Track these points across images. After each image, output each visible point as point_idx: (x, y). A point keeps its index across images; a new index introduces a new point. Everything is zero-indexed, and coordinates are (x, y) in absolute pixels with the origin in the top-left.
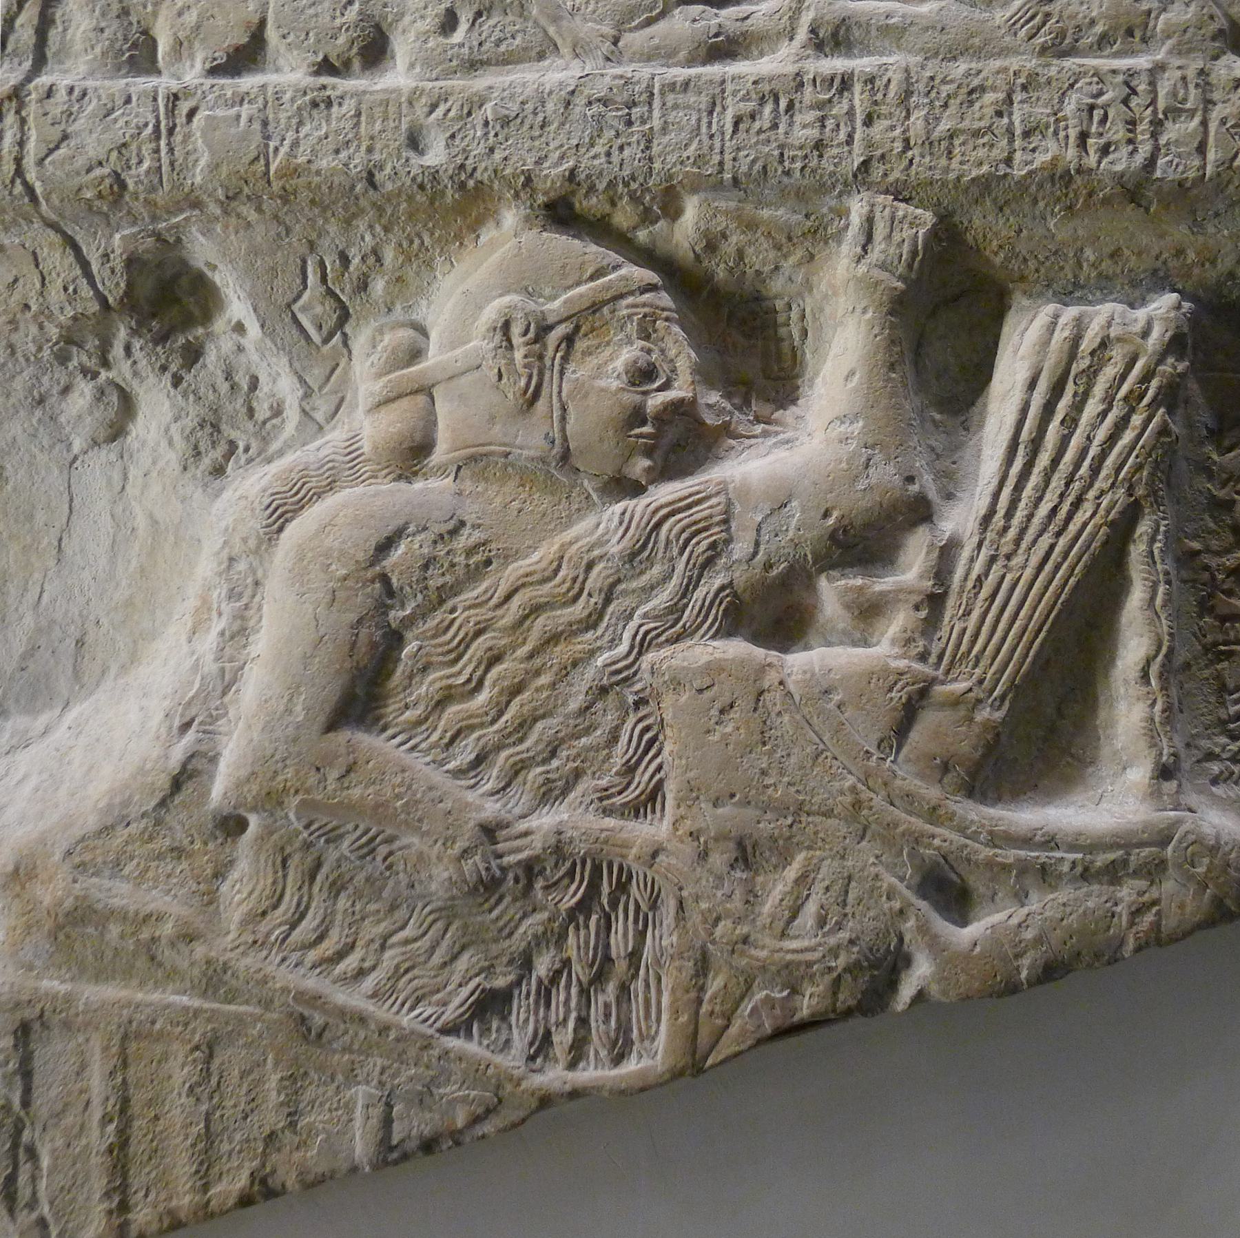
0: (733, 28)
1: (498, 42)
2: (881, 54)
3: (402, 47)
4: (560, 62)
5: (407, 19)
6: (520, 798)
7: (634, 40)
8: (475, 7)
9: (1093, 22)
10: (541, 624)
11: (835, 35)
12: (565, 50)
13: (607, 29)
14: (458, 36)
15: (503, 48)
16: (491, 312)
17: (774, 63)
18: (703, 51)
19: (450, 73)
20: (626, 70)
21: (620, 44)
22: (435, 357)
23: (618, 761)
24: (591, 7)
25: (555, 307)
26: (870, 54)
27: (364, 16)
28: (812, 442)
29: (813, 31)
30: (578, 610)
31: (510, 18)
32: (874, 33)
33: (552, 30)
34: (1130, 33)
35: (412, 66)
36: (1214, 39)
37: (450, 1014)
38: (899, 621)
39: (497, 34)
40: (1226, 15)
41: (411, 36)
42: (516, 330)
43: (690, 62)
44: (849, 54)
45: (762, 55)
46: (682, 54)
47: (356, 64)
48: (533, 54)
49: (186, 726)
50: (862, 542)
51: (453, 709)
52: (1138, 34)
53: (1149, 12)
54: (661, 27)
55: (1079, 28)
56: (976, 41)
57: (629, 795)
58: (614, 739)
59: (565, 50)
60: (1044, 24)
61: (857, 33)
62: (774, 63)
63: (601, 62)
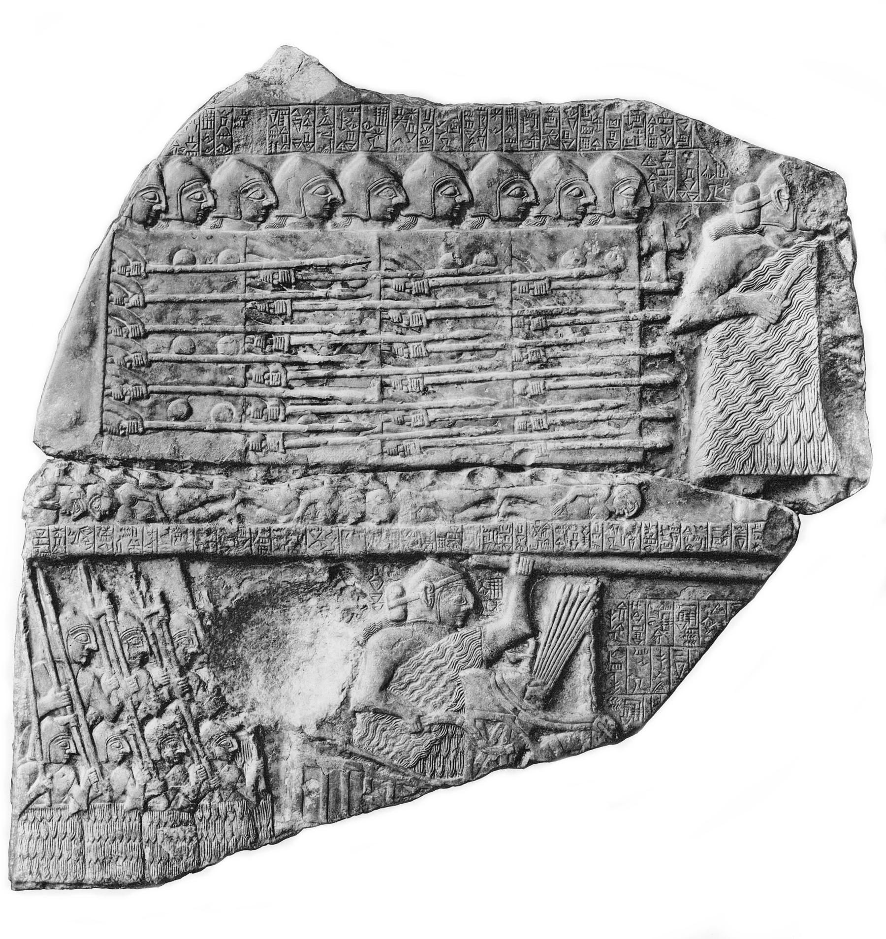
3: (401, 517)
6: (429, 707)
7: (458, 516)
10: (434, 664)
16: (422, 586)
17: (495, 521)
22: (409, 595)
23: (453, 699)
25: (437, 584)
28: (504, 617)
30: (443, 660)
37: (411, 763)
38: (525, 664)
42: (428, 590)
49: (343, 690)
50: (517, 642)
51: (411, 685)
57: (456, 707)
58: (451, 695)
62: (495, 521)
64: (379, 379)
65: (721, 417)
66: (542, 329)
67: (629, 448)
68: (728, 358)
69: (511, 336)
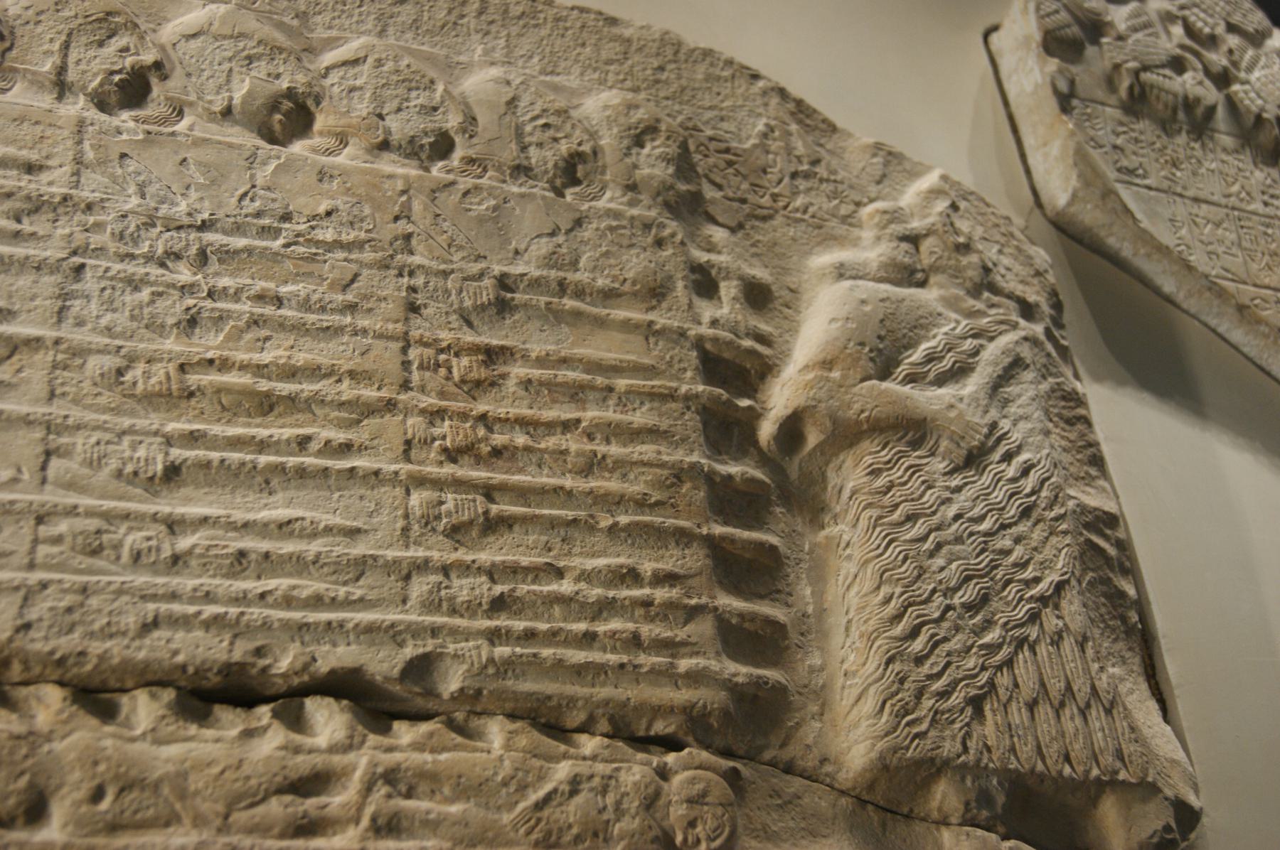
0: (314, 813)
1: (136, 812)
2: (422, 839)
4: (181, 830)
5: (65, 790)
7: (240, 817)
8: (121, 784)
9: (570, 827)
11: (389, 823)
12: (187, 821)
13: (220, 808)
14: (105, 805)
15: (139, 816)
18: (291, 830)
19: (94, 833)
20: (234, 839)
21: (231, 819)
24: (210, 791)
26: (414, 838)
27: (31, 785)
29: (374, 819)
31: (147, 794)
32: (417, 824)
33: (178, 806)
34: (596, 835)
35: (65, 825)
36: (652, 842)
39: (134, 807)
40: (660, 827)
41: (68, 802)
43: (282, 836)
44: (398, 838)
45: (334, 834)
46: (276, 831)
47: (20, 821)
48: (162, 821)
52: (601, 836)
53: (608, 821)
54: (260, 810)
55: (560, 830)
56: (490, 834)
59: (187, 821)
60: (537, 824)
61: (405, 824)
63: (213, 832)
64: (38, 434)
65: (899, 630)
66: (478, 383)
67: (695, 678)
68: (896, 506)
69: (405, 386)
